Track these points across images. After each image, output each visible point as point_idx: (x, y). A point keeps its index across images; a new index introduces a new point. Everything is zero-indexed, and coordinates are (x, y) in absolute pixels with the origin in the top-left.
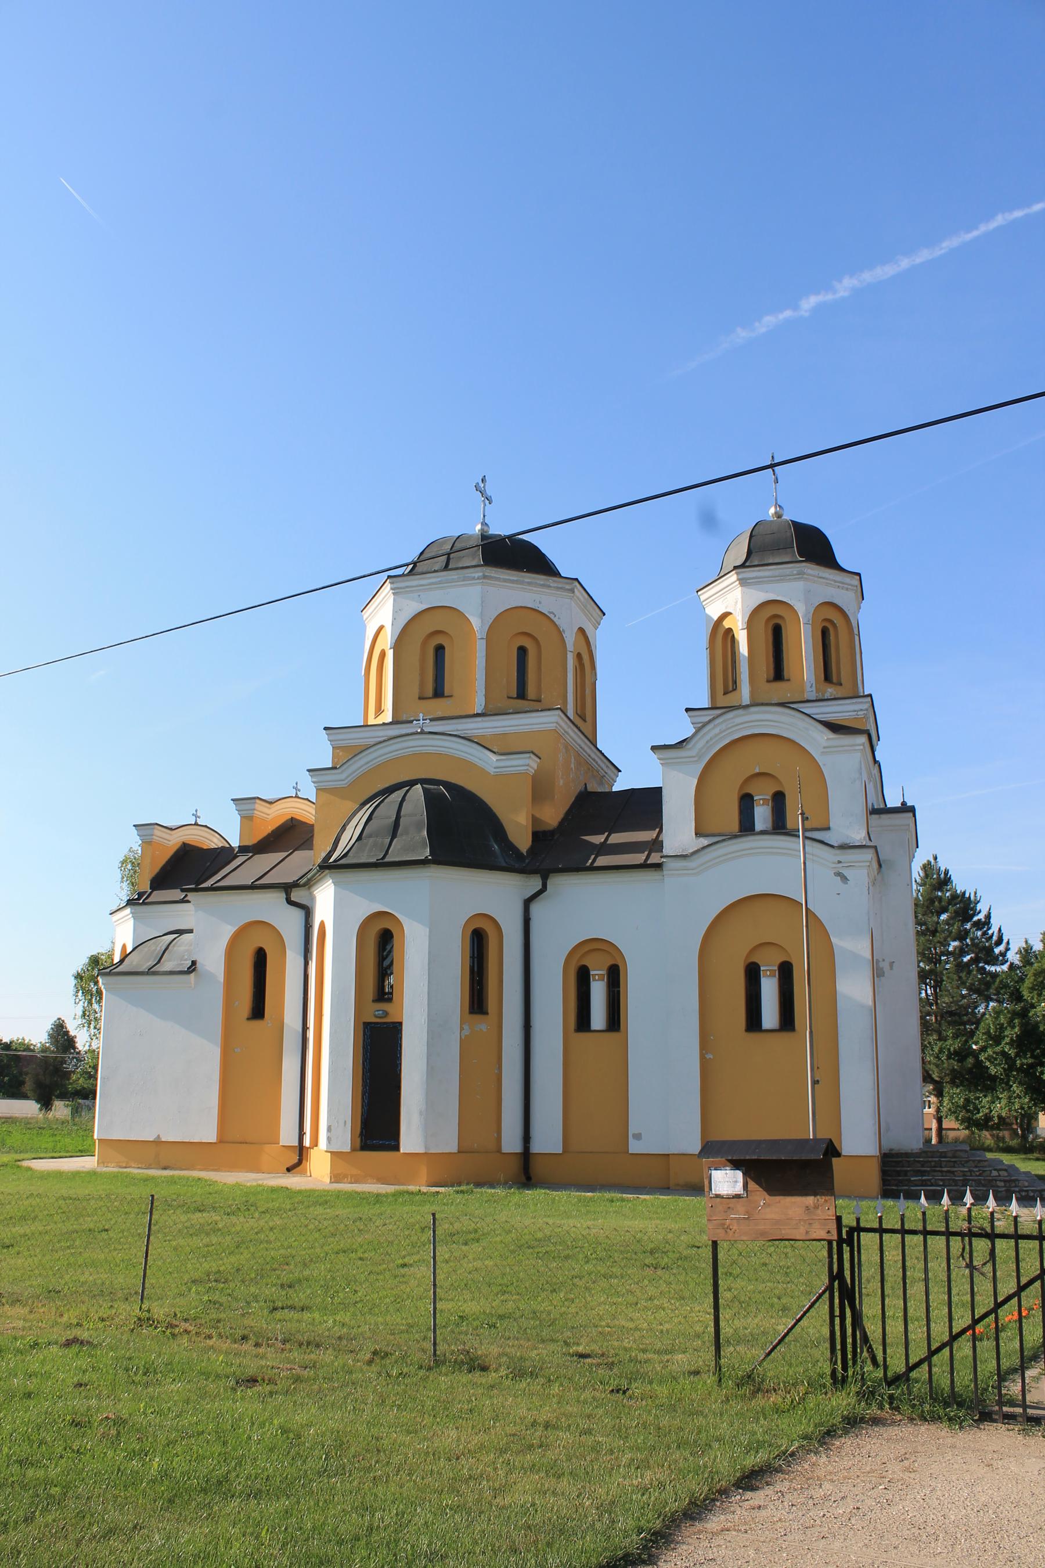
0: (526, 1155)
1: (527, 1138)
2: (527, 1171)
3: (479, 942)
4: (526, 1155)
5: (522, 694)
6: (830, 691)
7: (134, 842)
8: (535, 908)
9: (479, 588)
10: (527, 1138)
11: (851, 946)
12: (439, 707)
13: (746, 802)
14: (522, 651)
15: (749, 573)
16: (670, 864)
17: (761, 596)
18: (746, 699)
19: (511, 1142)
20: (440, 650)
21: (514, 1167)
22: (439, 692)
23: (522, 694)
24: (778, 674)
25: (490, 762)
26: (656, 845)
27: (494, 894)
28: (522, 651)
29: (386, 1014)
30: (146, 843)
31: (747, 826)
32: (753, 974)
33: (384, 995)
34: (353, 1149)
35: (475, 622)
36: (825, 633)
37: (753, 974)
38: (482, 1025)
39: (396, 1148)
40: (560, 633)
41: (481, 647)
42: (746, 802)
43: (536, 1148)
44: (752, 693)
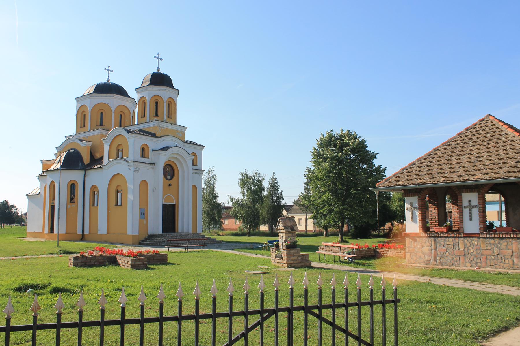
0: (83, 234)
1: (83, 230)
2: (83, 238)
3: (73, 187)
4: (83, 234)
5: (101, 125)
6: (156, 118)
7: (40, 165)
8: (86, 178)
9: (89, 100)
10: (83, 230)
11: (130, 186)
12: (84, 129)
13: (118, 151)
14: (102, 114)
15: (138, 90)
16: (104, 167)
17: (141, 96)
18: (136, 123)
19: (80, 231)
20: (85, 115)
21: (81, 237)
22: (84, 126)
23: (101, 125)
24: (145, 116)
25: (81, 143)
26: (102, 163)
27: (76, 176)
28: (102, 114)
29: (54, 203)
30: (43, 164)
31: (117, 157)
32: (117, 192)
33: (54, 200)
34: (48, 233)
35: (88, 108)
36: (157, 103)
37: (117, 192)
38: (73, 205)
39: (53, 233)
40: (110, 108)
41: (90, 114)
42: (118, 151)
43: (85, 233)
44: (138, 121)
